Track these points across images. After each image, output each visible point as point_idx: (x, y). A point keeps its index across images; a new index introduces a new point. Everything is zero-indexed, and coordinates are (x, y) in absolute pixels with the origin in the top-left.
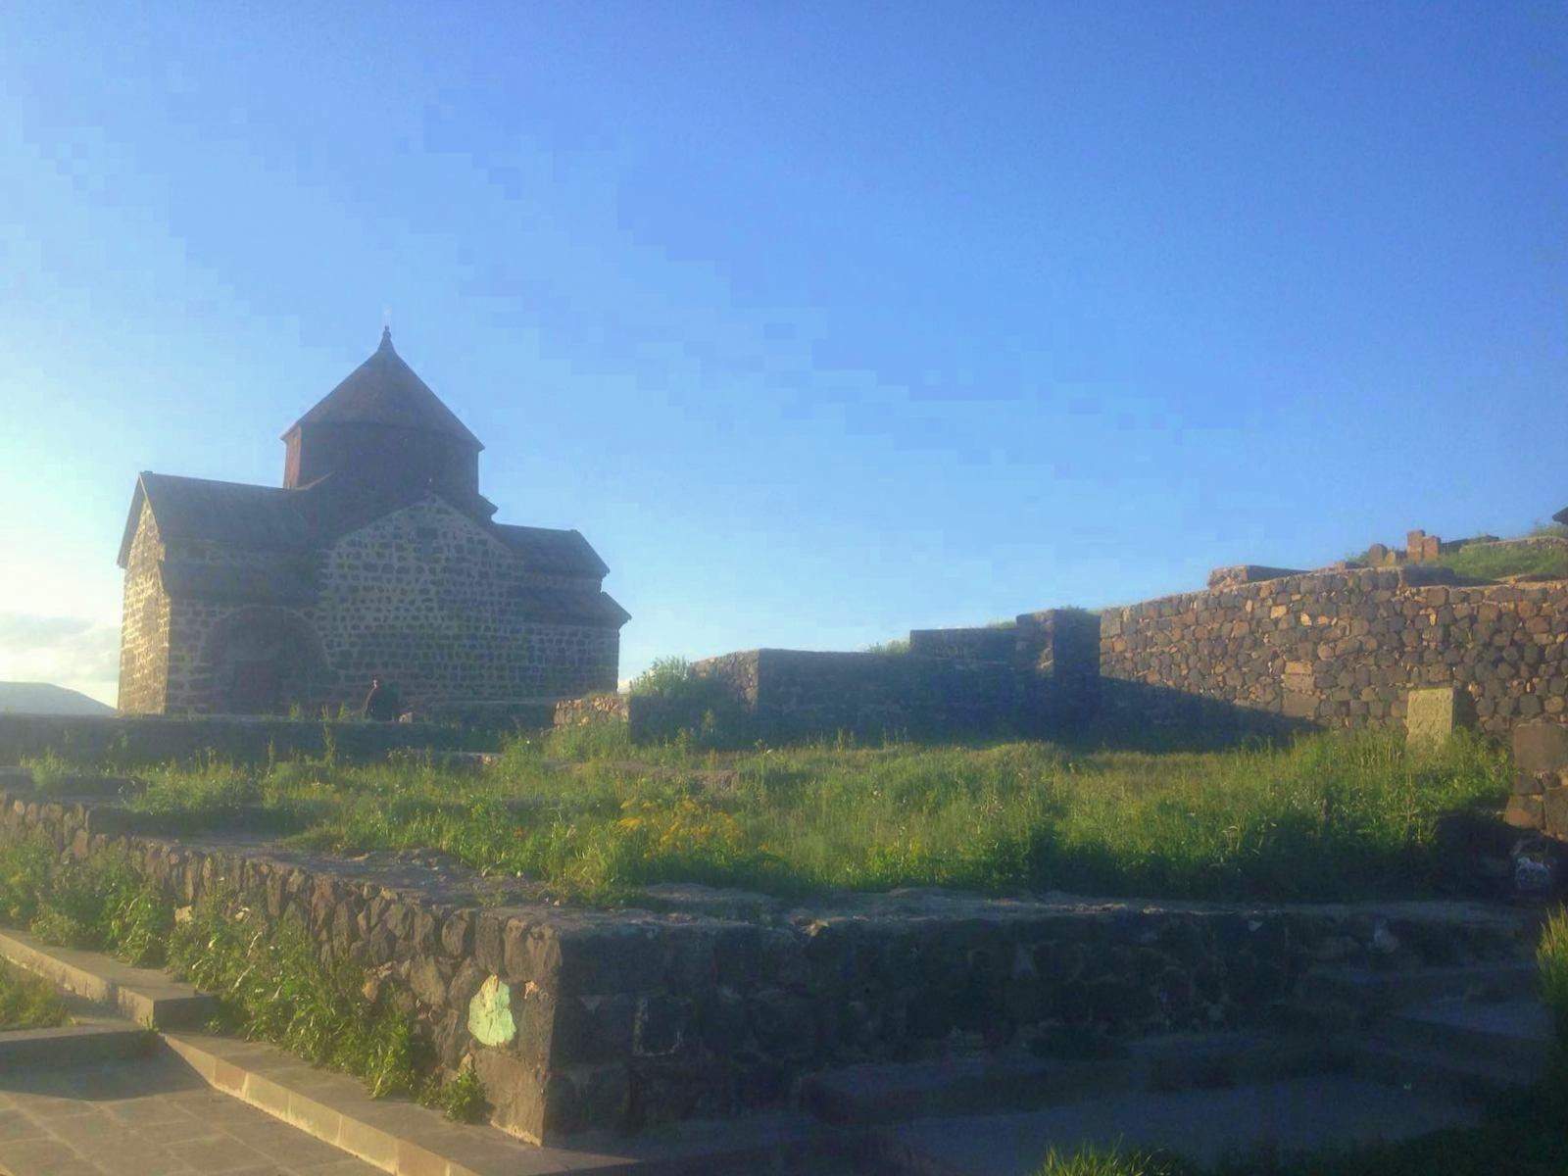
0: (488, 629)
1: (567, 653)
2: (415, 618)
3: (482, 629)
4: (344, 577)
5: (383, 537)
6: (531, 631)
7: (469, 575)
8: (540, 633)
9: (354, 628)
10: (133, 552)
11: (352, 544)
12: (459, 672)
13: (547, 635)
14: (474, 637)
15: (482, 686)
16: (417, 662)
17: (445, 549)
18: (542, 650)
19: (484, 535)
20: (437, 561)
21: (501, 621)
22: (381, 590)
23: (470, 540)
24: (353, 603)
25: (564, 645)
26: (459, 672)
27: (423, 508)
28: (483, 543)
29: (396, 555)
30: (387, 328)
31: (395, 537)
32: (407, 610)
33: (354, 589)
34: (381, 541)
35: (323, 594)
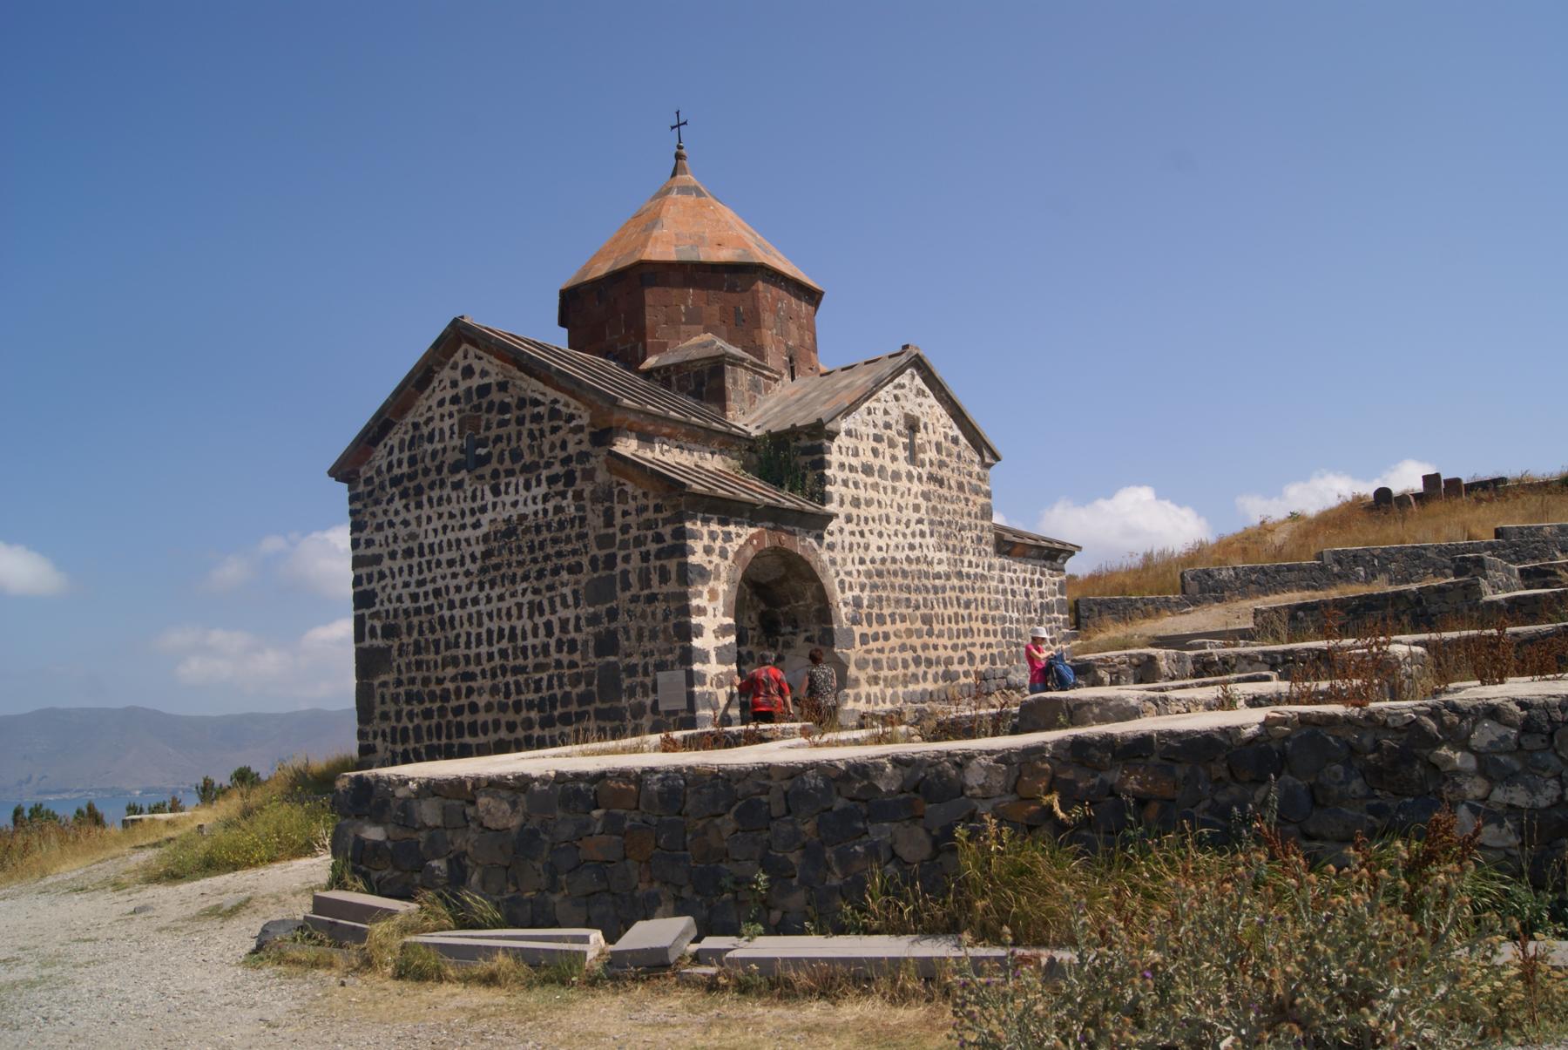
0: (970, 563)
1: (1032, 598)
2: (912, 547)
3: (966, 564)
4: (845, 483)
5: (875, 426)
6: (1003, 569)
7: (950, 488)
9: (862, 561)
10: (380, 456)
11: (849, 433)
14: (959, 575)
15: (973, 645)
16: (918, 613)
18: (1013, 593)
19: (956, 432)
20: (923, 465)
22: (879, 502)
23: (946, 436)
24: (858, 524)
26: (953, 626)
27: (902, 386)
28: (955, 441)
29: (888, 452)
31: (887, 426)
32: (904, 535)
33: (856, 502)
34: (875, 431)
35: (831, 508)
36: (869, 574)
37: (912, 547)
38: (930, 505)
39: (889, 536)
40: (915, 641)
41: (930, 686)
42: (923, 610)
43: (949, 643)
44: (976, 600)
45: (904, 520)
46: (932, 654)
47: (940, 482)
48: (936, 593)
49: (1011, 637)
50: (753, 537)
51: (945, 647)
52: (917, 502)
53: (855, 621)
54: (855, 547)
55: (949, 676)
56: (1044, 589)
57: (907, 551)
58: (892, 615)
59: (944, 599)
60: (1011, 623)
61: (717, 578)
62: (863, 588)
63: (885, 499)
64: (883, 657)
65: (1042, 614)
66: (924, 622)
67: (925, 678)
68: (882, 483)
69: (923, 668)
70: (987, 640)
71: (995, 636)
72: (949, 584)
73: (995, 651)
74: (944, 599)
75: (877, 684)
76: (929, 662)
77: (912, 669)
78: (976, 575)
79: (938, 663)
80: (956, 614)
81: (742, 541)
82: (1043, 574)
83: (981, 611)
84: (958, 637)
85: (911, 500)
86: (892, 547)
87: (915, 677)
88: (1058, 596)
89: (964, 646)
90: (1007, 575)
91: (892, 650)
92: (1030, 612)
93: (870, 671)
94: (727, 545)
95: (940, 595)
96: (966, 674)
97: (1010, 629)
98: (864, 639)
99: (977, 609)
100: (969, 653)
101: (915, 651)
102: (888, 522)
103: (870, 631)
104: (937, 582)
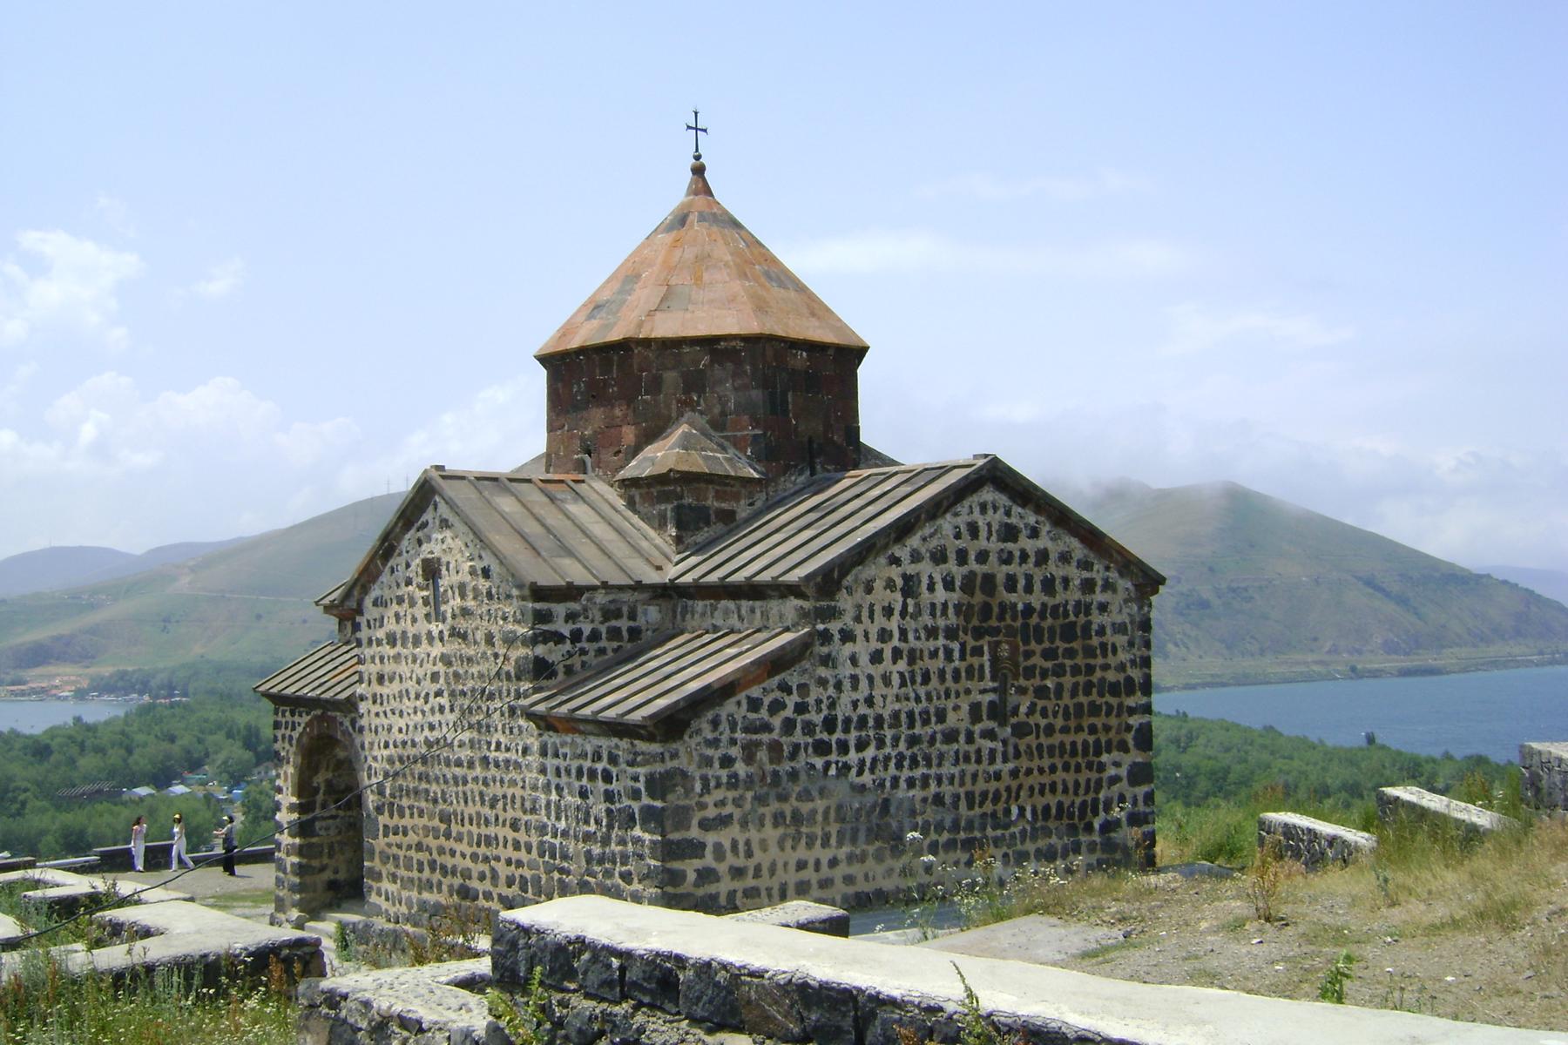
0: (498, 744)
3: (493, 747)
7: (475, 643)
8: (556, 755)
9: (386, 746)
11: (375, 604)
12: (474, 829)
13: (565, 756)
14: (485, 761)
15: (497, 859)
17: (450, 591)
21: (511, 732)
25: (585, 781)
26: (474, 829)
30: (698, 158)
32: (423, 712)
36: (390, 761)
37: (432, 727)
38: (451, 670)
39: (409, 714)
40: (430, 841)
41: (442, 899)
42: (441, 806)
43: (468, 851)
44: (504, 797)
45: (423, 695)
46: (449, 861)
47: (464, 637)
48: (456, 784)
49: (553, 856)
50: (307, 725)
51: (463, 856)
52: (435, 669)
53: (379, 810)
54: (380, 729)
55: (465, 893)
56: (614, 786)
57: (427, 732)
58: (411, 808)
59: (465, 793)
60: (555, 836)
61: (288, 762)
62: (386, 775)
63: (403, 669)
64: (401, 853)
65: (610, 827)
66: (441, 821)
67: (440, 891)
68: (404, 652)
69: (437, 876)
70: (515, 855)
71: (529, 852)
72: (471, 775)
73: (528, 873)
74: (465, 793)
75: (395, 882)
76: (444, 871)
77: (427, 873)
78: (507, 762)
79: (454, 873)
80: (478, 814)
81: (300, 729)
82: (613, 759)
83: (510, 814)
84: (479, 845)
85: (429, 668)
86: (411, 728)
87: (429, 886)
88: (646, 800)
89: (486, 859)
90: (551, 762)
91: (409, 847)
92: (587, 822)
93: (391, 867)
94: (293, 734)
95: (460, 788)
96: (488, 896)
97: (553, 846)
98: (386, 826)
99: (505, 810)
100: (493, 870)
101: (431, 854)
102: (409, 699)
103: (391, 823)
104: (458, 771)
